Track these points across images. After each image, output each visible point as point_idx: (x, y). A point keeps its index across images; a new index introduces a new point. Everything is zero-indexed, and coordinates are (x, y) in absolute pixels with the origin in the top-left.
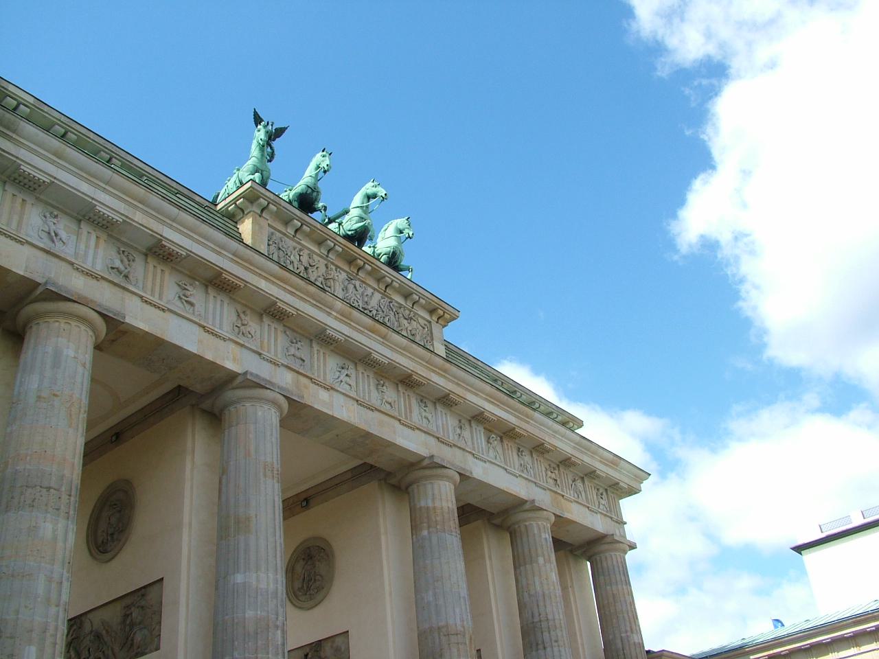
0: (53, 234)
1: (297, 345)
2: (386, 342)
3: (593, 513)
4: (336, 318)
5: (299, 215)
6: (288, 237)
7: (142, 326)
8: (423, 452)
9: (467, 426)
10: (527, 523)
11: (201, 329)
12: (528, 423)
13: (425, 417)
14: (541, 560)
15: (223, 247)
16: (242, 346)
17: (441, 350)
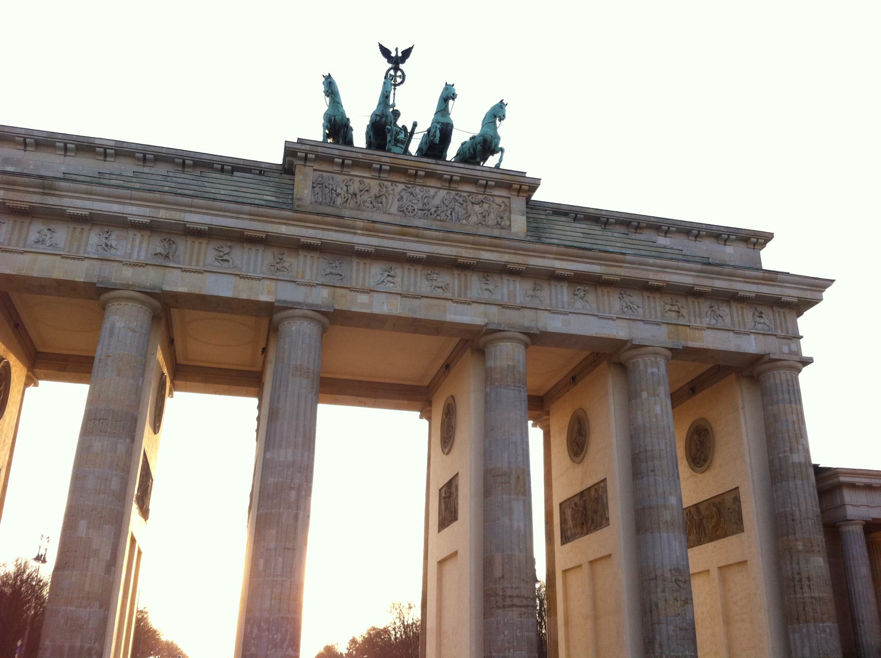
0: (104, 246)
1: (334, 265)
2: (422, 240)
3: (741, 335)
4: (363, 235)
5: (337, 154)
6: (337, 173)
7: (182, 289)
8: (479, 321)
9: (546, 286)
10: (634, 361)
11: (237, 278)
12: (621, 267)
13: (486, 290)
14: (644, 395)
16: (277, 280)
17: (519, 224)
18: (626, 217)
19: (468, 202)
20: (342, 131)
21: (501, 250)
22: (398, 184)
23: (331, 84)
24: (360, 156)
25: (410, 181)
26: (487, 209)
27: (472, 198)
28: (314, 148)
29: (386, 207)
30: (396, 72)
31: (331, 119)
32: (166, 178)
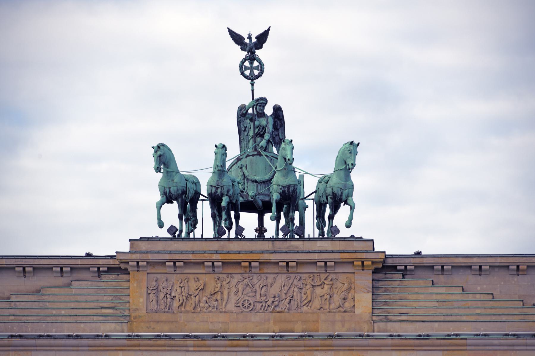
5: (168, 259)
15: (78, 346)
18: (503, 261)
19: (308, 287)
20: (180, 200)
21: (334, 348)
22: (234, 275)
23: (162, 157)
24: (191, 256)
25: (246, 271)
26: (329, 291)
27: (313, 280)
28: (144, 256)
29: (222, 303)
30: (251, 63)
31: (166, 192)
32: (10, 304)
